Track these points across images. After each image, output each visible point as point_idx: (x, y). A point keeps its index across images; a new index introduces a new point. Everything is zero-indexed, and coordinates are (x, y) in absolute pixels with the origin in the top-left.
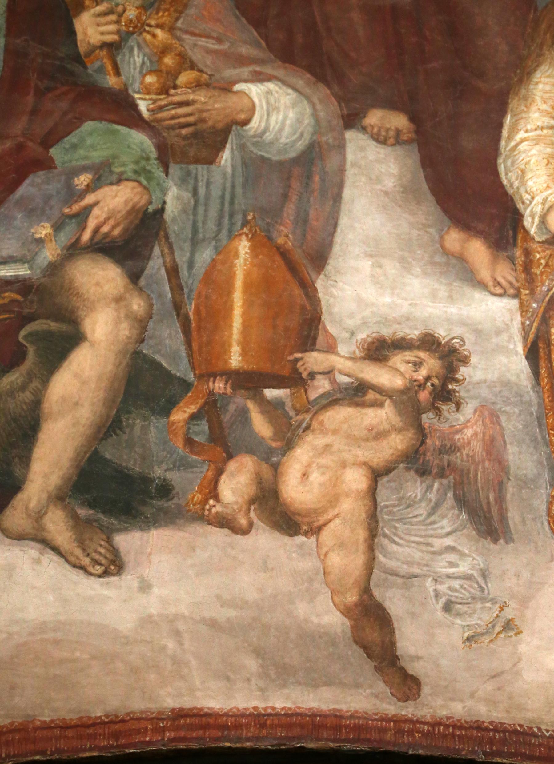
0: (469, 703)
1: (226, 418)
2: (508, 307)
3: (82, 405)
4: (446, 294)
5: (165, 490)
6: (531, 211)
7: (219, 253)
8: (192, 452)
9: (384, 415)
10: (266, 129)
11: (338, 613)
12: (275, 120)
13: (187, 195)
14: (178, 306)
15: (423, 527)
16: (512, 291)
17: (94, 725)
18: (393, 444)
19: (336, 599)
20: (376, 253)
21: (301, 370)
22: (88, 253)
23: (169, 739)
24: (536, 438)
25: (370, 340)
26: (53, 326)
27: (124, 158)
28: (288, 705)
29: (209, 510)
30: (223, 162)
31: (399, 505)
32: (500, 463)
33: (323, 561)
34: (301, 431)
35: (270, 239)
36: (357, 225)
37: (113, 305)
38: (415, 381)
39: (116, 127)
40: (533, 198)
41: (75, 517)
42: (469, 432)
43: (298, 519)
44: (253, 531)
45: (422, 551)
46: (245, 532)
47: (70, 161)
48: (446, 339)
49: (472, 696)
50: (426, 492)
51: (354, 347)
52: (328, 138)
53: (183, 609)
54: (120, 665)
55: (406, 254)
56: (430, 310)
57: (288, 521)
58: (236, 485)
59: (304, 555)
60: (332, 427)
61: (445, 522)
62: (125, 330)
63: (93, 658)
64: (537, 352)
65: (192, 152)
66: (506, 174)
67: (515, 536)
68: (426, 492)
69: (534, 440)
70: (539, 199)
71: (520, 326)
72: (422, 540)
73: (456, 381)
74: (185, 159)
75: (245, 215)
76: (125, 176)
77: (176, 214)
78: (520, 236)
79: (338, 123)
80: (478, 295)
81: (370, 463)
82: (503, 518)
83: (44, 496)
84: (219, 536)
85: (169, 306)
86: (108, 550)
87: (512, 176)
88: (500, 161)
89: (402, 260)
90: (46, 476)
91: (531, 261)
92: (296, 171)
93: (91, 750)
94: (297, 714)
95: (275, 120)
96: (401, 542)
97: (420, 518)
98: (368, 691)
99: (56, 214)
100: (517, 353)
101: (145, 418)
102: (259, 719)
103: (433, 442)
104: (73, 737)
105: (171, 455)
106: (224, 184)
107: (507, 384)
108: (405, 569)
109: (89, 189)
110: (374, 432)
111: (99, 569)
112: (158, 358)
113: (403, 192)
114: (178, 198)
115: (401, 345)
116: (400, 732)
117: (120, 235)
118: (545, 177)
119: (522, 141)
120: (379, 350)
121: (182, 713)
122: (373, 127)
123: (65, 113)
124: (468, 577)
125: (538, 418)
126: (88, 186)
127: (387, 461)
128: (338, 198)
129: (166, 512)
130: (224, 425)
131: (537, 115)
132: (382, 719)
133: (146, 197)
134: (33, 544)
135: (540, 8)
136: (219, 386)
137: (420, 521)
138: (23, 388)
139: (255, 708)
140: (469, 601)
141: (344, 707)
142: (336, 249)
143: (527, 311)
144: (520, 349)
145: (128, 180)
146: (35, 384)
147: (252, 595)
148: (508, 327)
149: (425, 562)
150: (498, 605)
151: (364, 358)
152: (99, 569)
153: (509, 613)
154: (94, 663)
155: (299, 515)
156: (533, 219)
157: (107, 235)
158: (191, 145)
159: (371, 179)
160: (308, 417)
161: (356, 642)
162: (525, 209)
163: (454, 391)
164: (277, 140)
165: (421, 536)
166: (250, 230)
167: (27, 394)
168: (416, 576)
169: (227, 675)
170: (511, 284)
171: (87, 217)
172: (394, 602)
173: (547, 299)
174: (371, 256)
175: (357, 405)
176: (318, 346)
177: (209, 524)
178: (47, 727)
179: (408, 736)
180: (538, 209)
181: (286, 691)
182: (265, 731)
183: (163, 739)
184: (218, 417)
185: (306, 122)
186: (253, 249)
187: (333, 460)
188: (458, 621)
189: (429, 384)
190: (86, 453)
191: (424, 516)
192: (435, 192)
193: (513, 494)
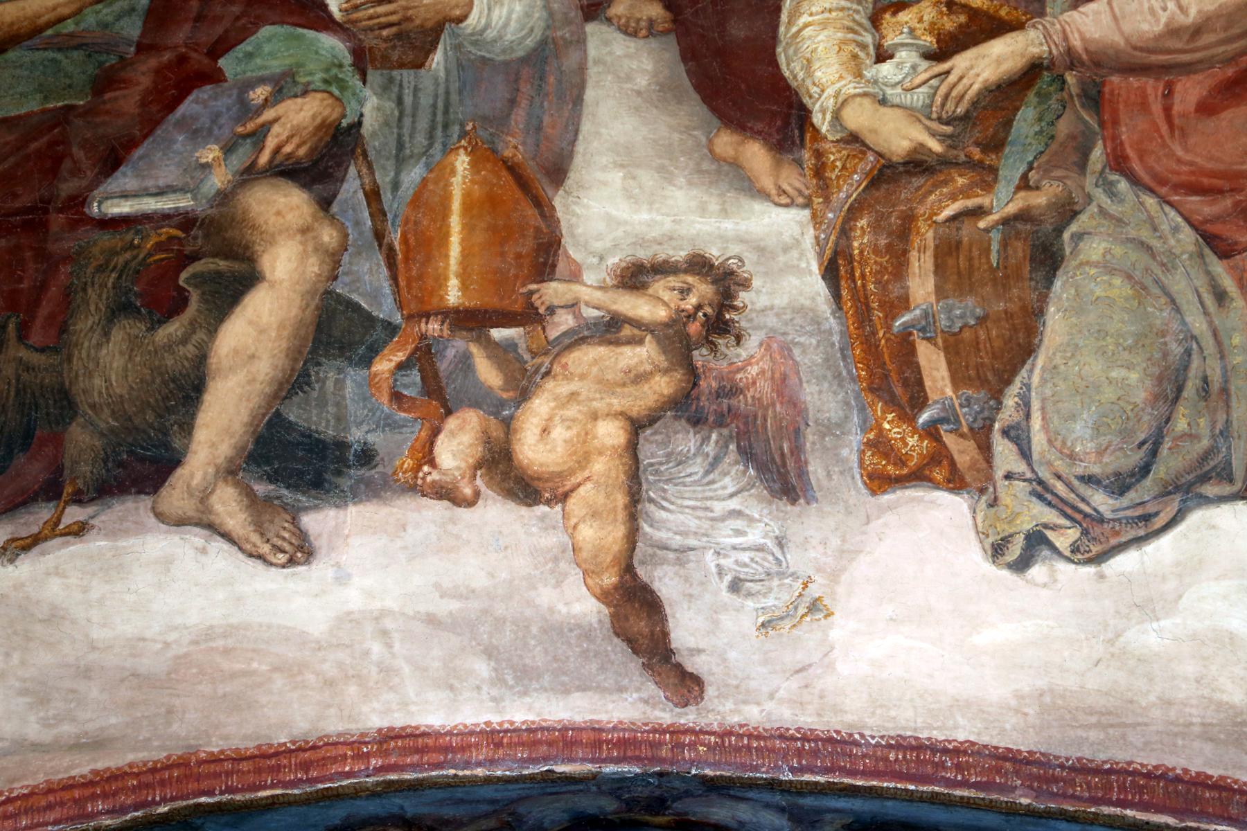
0: (769, 706)
1: (443, 366)
2: (798, 219)
3: (259, 358)
4: (718, 207)
5: (367, 456)
6: (822, 106)
7: (431, 171)
8: (400, 409)
9: (644, 354)
10: (487, 26)
11: (594, 600)
12: (499, 15)
13: (390, 105)
14: (379, 235)
15: (700, 488)
16: (800, 200)
17: (277, 754)
18: (657, 388)
19: (589, 581)
20: (627, 160)
21: (538, 303)
22: (266, 177)
23: (375, 768)
24: (840, 374)
25: (623, 264)
26: (222, 264)
27: (311, 66)
28: (531, 717)
29: (423, 479)
30: (434, 66)
31: (668, 462)
32: (795, 405)
33: (572, 537)
34: (538, 378)
35: (494, 151)
36: (603, 130)
37: (298, 237)
39: (300, 30)
40: (823, 91)
41: (249, 494)
42: (754, 370)
43: (539, 485)
44: (480, 502)
45: (699, 518)
46: (470, 503)
47: (244, 72)
48: (720, 260)
50: (701, 445)
51: (604, 275)
52: (565, 33)
53: (391, 604)
54: (310, 678)
55: (667, 162)
56: (698, 226)
57: (524, 488)
58: (456, 448)
59: (546, 529)
60: (579, 371)
61: (727, 480)
62: (314, 267)
63: (276, 669)
64: (837, 270)
65: (395, 56)
66: (788, 65)
67: (818, 495)
68: (701, 445)
69: (838, 376)
70: (830, 91)
71: (813, 241)
72: (698, 504)
74: (386, 63)
75: (462, 125)
76: (312, 87)
77: (377, 127)
78: (808, 136)
79: (576, 15)
80: (758, 206)
81: (629, 413)
82: (802, 473)
83: (211, 470)
84: (437, 509)
85: (369, 234)
86: (294, 534)
88: (779, 50)
89: (661, 169)
90: (213, 445)
92: (526, 72)
93: (273, 786)
94: (542, 729)
95: (499, 15)
96: (672, 507)
97: (696, 478)
98: (635, 695)
99: (226, 132)
101: (340, 371)
102: (494, 737)
103: (708, 384)
104: (249, 772)
105: (374, 414)
106: (436, 90)
107: (800, 310)
108: (677, 541)
109: (266, 104)
110: (632, 375)
111: (282, 558)
112: (355, 297)
114: (378, 109)
115: (662, 269)
116: (680, 746)
117: (306, 155)
118: (837, 66)
119: (806, 26)
120: (635, 277)
121: (392, 734)
122: (619, 18)
123: (238, 18)
124: (760, 549)
125: (842, 350)
126: (266, 100)
127: (650, 409)
128: (578, 101)
129: (368, 483)
130: (441, 375)
132: (654, 731)
133: (338, 110)
134: (197, 530)
136: (433, 327)
137: (695, 481)
138: (184, 341)
139: (488, 723)
140: (763, 577)
141: (604, 717)
142: (578, 160)
143: (821, 223)
144: (815, 267)
145: (315, 91)
146: (200, 335)
147: (480, 581)
148: (797, 242)
150: (801, 581)
151: (618, 287)
152: (282, 558)
153: (814, 591)
154: (276, 676)
155: (539, 479)
156: (824, 114)
157: (289, 156)
158: (394, 47)
159: (619, 77)
160: (547, 361)
161: (617, 635)
162: (814, 104)
163: (733, 321)
164: (501, 38)
165: (696, 499)
166: (469, 143)
167: (190, 347)
168: (692, 549)
169: (450, 681)
170: (800, 192)
171: (265, 136)
172: (665, 583)
173: (846, 207)
174: (622, 166)
175: (610, 343)
176: (557, 276)
177: (424, 496)
178: (214, 759)
179: (689, 751)
181: (528, 700)
182: (501, 752)
183: (368, 768)
184: (433, 365)
185: (537, 15)
186: (474, 165)
187: (580, 411)
188: (750, 603)
190: (264, 415)
191: (700, 474)
192: (698, 88)
193: (814, 443)
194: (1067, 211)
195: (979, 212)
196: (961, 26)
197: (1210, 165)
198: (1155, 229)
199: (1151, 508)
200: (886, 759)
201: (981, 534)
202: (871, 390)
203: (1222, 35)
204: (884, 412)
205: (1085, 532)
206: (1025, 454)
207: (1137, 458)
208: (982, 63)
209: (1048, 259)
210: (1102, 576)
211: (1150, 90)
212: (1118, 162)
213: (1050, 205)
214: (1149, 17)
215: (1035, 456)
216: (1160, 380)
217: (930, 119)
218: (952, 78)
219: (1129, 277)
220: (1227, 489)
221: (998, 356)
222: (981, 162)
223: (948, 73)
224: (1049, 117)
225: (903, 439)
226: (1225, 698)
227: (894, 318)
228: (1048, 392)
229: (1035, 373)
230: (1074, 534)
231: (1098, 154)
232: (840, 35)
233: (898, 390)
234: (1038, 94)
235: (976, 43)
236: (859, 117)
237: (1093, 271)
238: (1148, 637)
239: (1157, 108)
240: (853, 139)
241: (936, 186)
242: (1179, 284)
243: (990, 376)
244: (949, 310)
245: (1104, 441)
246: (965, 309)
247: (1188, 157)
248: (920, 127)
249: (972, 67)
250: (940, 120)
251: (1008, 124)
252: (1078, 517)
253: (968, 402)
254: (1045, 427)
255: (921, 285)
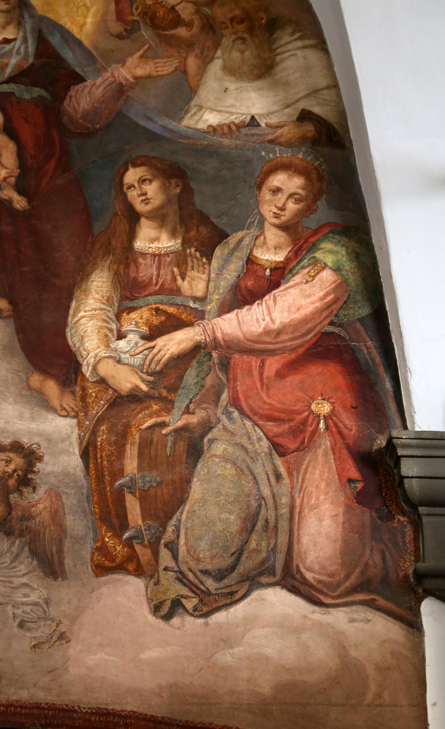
2: (70, 424)
4: (29, 415)
6: (87, 362)
15: (7, 571)
16: (73, 414)
24: (86, 510)
32: (61, 527)
38: (6, 472)
40: (88, 354)
42: (41, 506)
45: (6, 587)
48: (28, 445)
49: (35, 685)
50: (10, 547)
55: (4, 389)
56: (18, 426)
61: (22, 567)
66: (72, 338)
67: (69, 576)
68: (10, 547)
69: (84, 511)
70: (92, 354)
71: (77, 436)
72: (6, 579)
73: (34, 472)
78: (79, 378)
80: (50, 416)
82: (61, 564)
87: (75, 339)
88: (68, 330)
91: (86, 394)
97: (6, 565)
100: (74, 454)
107: (67, 474)
113: (3, 349)
118: (97, 341)
124: (36, 604)
125: (87, 497)
131: (92, 301)
135: (95, 235)
137: (5, 567)
140: (36, 620)
143: (82, 427)
144: (77, 451)
149: (7, 594)
150: (55, 623)
153: (62, 628)
156: (88, 367)
162: (83, 361)
163: (32, 479)
165: (5, 577)
170: (73, 409)
173: (96, 419)
180: (92, 361)
188: (28, 634)
189: (15, 474)
191: (8, 563)
193: (69, 548)
194: (207, 426)
195: (163, 425)
196: (161, 322)
197: (279, 406)
198: (250, 439)
199: (234, 588)
200: (90, 720)
201: (149, 600)
202: (101, 519)
203: (291, 336)
204: (106, 532)
205: (201, 600)
206: (175, 557)
207: (230, 561)
208: (171, 343)
209: (195, 452)
210: (207, 624)
211: (253, 363)
212: (235, 402)
213: (199, 424)
214: (256, 324)
215: (180, 559)
216: (245, 520)
217: (142, 372)
218: (155, 351)
219: (234, 464)
220: (272, 580)
221: (166, 504)
222: (166, 398)
223: (153, 347)
224: (203, 374)
225: (114, 547)
226: (261, 690)
227: (116, 481)
228: (189, 525)
229: (184, 514)
230: (195, 601)
231: (225, 396)
232: (99, 324)
233: (115, 521)
234: (198, 362)
235: (168, 332)
236: (107, 369)
237: (217, 460)
238: (226, 657)
239: (256, 373)
240: (102, 381)
241: (142, 410)
242: (259, 470)
243: (161, 514)
244: (143, 477)
245: (214, 552)
246: (153, 476)
247: (268, 401)
248: (137, 376)
249: (165, 345)
250: (147, 373)
251: (181, 377)
252: (198, 592)
253: (149, 528)
254: (186, 544)
255: (131, 465)
